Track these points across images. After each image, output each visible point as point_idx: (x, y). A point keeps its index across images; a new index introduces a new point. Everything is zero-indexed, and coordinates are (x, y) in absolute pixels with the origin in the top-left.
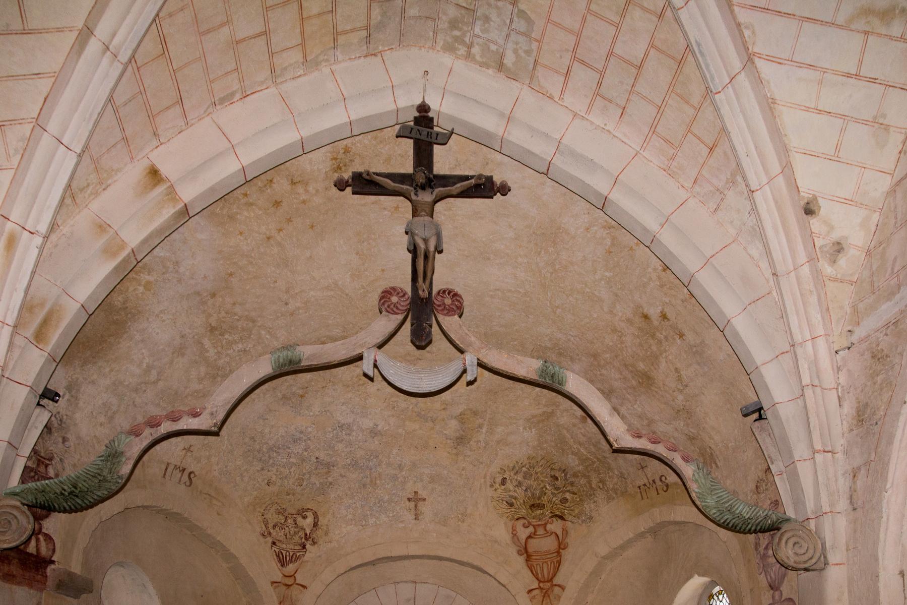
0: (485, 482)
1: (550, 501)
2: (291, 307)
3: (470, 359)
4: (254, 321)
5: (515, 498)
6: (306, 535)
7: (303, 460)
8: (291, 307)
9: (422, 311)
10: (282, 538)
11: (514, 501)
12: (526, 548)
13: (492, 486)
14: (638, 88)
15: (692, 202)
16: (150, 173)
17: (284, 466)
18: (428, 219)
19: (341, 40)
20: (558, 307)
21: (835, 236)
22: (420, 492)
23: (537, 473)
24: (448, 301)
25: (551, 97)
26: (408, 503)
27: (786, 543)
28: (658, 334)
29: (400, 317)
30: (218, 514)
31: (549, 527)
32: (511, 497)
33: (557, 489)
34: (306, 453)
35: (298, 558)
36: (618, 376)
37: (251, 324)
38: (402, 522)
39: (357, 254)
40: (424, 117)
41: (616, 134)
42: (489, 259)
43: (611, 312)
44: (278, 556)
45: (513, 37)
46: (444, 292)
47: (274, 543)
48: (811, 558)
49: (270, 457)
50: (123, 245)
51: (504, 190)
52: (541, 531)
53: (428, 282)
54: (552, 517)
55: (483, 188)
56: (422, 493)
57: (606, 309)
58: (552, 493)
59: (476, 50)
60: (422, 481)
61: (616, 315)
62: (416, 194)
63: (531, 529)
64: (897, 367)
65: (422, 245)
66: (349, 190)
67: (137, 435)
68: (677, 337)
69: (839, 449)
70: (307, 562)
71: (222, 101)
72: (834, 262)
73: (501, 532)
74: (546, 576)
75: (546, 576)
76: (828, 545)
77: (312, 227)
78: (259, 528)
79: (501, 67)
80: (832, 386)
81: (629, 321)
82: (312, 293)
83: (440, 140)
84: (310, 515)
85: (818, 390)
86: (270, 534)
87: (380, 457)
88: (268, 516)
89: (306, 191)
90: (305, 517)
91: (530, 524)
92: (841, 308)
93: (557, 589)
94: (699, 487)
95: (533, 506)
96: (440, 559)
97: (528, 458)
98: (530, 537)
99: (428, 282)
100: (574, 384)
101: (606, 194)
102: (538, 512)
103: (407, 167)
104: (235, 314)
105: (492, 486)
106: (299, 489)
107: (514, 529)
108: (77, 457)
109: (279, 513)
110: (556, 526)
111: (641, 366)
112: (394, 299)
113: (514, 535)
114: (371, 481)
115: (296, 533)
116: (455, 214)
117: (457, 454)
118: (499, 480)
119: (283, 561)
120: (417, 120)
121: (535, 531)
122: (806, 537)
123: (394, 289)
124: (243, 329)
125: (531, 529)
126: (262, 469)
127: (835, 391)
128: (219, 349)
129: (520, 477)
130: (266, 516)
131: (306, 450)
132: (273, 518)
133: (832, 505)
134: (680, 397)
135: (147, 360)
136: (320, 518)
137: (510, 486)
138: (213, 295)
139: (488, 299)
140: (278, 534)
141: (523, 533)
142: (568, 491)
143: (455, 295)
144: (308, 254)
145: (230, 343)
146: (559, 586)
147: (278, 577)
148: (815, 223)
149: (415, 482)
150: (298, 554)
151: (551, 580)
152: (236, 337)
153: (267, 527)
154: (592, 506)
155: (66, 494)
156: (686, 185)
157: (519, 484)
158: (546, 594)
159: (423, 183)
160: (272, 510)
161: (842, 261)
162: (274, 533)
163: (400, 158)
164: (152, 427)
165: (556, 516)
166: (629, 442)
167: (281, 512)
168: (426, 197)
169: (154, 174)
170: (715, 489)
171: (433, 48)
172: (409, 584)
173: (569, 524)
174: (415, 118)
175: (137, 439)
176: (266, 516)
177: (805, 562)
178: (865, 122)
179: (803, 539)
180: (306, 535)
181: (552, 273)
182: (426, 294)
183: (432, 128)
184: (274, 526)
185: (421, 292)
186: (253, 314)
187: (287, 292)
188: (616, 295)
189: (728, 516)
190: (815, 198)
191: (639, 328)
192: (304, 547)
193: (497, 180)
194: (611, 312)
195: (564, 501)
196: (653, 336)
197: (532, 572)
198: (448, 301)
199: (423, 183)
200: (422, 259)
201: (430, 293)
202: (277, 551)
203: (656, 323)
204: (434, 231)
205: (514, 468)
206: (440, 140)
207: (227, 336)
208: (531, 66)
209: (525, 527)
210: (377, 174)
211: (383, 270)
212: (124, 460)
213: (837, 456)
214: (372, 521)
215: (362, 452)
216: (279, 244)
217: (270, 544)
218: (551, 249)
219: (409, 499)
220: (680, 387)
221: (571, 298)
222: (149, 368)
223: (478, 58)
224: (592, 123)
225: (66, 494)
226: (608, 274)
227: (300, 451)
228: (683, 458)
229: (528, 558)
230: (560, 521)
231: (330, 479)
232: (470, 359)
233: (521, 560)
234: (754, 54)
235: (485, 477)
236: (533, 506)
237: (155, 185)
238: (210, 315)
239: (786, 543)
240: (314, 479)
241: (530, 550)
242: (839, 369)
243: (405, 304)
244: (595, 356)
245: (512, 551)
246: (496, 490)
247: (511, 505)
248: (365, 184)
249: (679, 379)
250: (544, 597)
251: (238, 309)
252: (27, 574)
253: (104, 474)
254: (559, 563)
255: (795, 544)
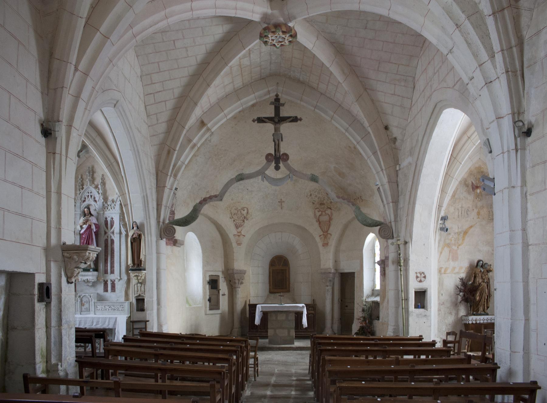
24: (285, 157)
52: (324, 213)
55: (295, 119)
63: (320, 213)
73: (311, 214)
84: (245, 209)
103: (273, 115)
110: (329, 212)
112: (270, 157)
113: (315, 215)
118: (309, 194)
119: (237, 227)
120: (275, 100)
125: (320, 213)
129: (316, 193)
132: (234, 211)
137: (313, 196)
140: (235, 217)
141: (318, 214)
147: (236, 233)
157: (316, 196)
163: (270, 112)
198: (285, 157)
210: (264, 118)
229: (320, 223)
233: (317, 224)
241: (320, 220)
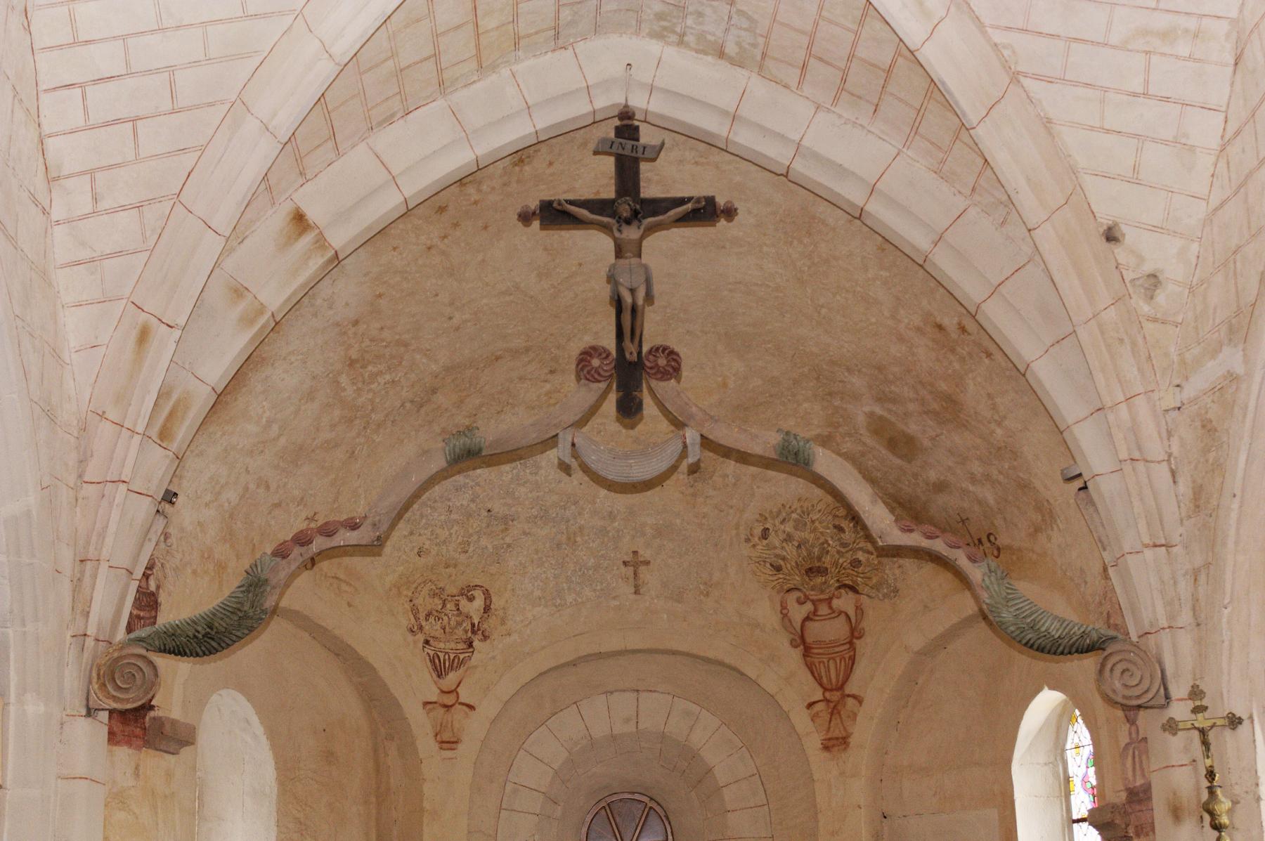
0: (738, 534)
1: (836, 564)
2: (455, 321)
3: (691, 435)
4: (406, 345)
5: (784, 559)
6: (473, 625)
7: (470, 515)
8: (455, 321)
9: (630, 372)
10: (439, 633)
11: (782, 563)
12: (802, 637)
13: (748, 540)
14: (890, 88)
15: (973, 212)
16: (294, 218)
17: (442, 527)
18: (634, 261)
19: (522, 43)
20: (822, 306)
21: (1148, 268)
22: (641, 552)
23: (813, 522)
24: (662, 362)
25: (786, 86)
26: (623, 569)
27: (1112, 670)
28: (959, 349)
29: (603, 385)
30: (349, 605)
31: (835, 603)
32: (777, 556)
33: (844, 545)
34: (473, 506)
35: (461, 663)
36: (912, 395)
37: (402, 349)
38: (614, 598)
39: (546, 249)
40: (627, 124)
41: (872, 129)
42: (723, 247)
43: (893, 317)
44: (432, 661)
45: (733, 31)
46: (657, 349)
47: (427, 642)
48: (1146, 691)
49: (422, 516)
50: (261, 309)
51: (730, 213)
52: (823, 610)
53: (637, 341)
54: (839, 588)
55: (705, 212)
56: (645, 554)
57: (886, 314)
58: (838, 552)
59: (690, 38)
60: (644, 534)
61: (900, 321)
62: (620, 231)
63: (809, 607)
64: (1225, 446)
65: (628, 299)
66: (536, 224)
67: (284, 557)
68: (984, 355)
69: (1176, 539)
70: (475, 667)
71: (380, 124)
72: (1152, 298)
73: (765, 611)
74: (834, 680)
75: (834, 680)
76: (1169, 673)
77: (486, 228)
78: (406, 620)
79: (721, 54)
80: (1161, 458)
81: (918, 329)
82: (485, 301)
83: (647, 155)
84: (478, 594)
85: (1140, 466)
86: (421, 628)
87: (581, 503)
88: (419, 601)
89: (479, 191)
90: (471, 599)
91: (807, 598)
92: (1166, 355)
93: (850, 701)
94: (991, 597)
95: (810, 571)
96: (674, 653)
97: (799, 500)
98: (807, 619)
99: (637, 341)
100: (825, 462)
101: (861, 205)
102: (819, 580)
103: (609, 193)
104: (383, 340)
105: (748, 540)
106: (463, 557)
107: (784, 607)
108: (179, 556)
109: (435, 595)
110: (845, 602)
111: (943, 386)
112: (596, 362)
113: (785, 615)
114: (569, 539)
115: (459, 624)
116: (666, 249)
117: (694, 495)
118: (758, 531)
119: (440, 669)
120: (619, 132)
121: (816, 610)
122: (1140, 662)
123: (594, 348)
124: (392, 357)
125: (809, 607)
126: (411, 533)
127: (1165, 463)
128: (360, 385)
129: (789, 528)
130: (415, 602)
131: (473, 501)
132: (425, 602)
133: (1172, 617)
134: (999, 431)
135: (268, 414)
136: (494, 599)
137: (774, 540)
138: (356, 323)
139: (726, 293)
140: (433, 627)
141: (798, 613)
142: (861, 549)
143: (672, 354)
144: (480, 257)
145: (374, 376)
146: (854, 697)
147: (433, 695)
148: (1120, 253)
149: (633, 537)
150: (462, 657)
151: (841, 688)
152: (382, 367)
153: (417, 619)
154: (897, 572)
155: (200, 636)
156: (963, 191)
157: (789, 538)
158: (835, 710)
159: (630, 206)
160: (425, 591)
161: (1161, 297)
162: (427, 628)
163: (597, 177)
164: (302, 545)
165: (845, 586)
166: (897, 537)
167: (437, 593)
168: (631, 233)
169: (300, 220)
170: (1013, 599)
171: (637, 32)
172: (627, 695)
173: (864, 599)
174: (617, 128)
175: (284, 562)
176: (415, 602)
177: (1138, 697)
178: (1165, 142)
179: (1135, 664)
180: (473, 625)
181: (809, 268)
182: (635, 357)
183: (638, 140)
184: (428, 615)
185: (628, 356)
186: (406, 337)
187: (451, 304)
188: (898, 299)
189: (1030, 635)
190: (1116, 224)
191: (934, 340)
192: (470, 645)
193: (721, 201)
194: (893, 317)
195: (856, 563)
196: (953, 350)
197: (812, 673)
198: (662, 362)
199: (630, 206)
200: (627, 318)
201: (640, 353)
202: (432, 653)
203: (954, 336)
204: (643, 279)
205: (779, 512)
206: (647, 155)
207: (370, 368)
208: (759, 58)
209: (800, 603)
210: (571, 202)
211: (580, 265)
212: (268, 589)
213: (1175, 550)
214: (570, 599)
215: (555, 498)
216: (443, 253)
217: (420, 645)
218: (806, 240)
219: (625, 563)
220: (996, 417)
221: (838, 297)
222: (270, 422)
223: (692, 45)
224: (840, 116)
225: (200, 636)
226: (884, 274)
227: (465, 503)
228: (969, 558)
229: (807, 651)
230: (851, 594)
231: (508, 540)
232: (691, 435)
233: (796, 655)
234: (1018, 73)
235: (737, 527)
236: (810, 571)
237: (300, 234)
238: (350, 346)
239: (1112, 670)
240: (484, 542)
241: (809, 640)
242: (1170, 434)
243: (608, 367)
244: (880, 368)
245: (782, 642)
246: (754, 546)
247: (778, 569)
248: (554, 215)
249: (994, 407)
250: (832, 714)
251: (386, 334)
252: (128, 729)
253: (246, 608)
254: (853, 660)
255: (1123, 672)
